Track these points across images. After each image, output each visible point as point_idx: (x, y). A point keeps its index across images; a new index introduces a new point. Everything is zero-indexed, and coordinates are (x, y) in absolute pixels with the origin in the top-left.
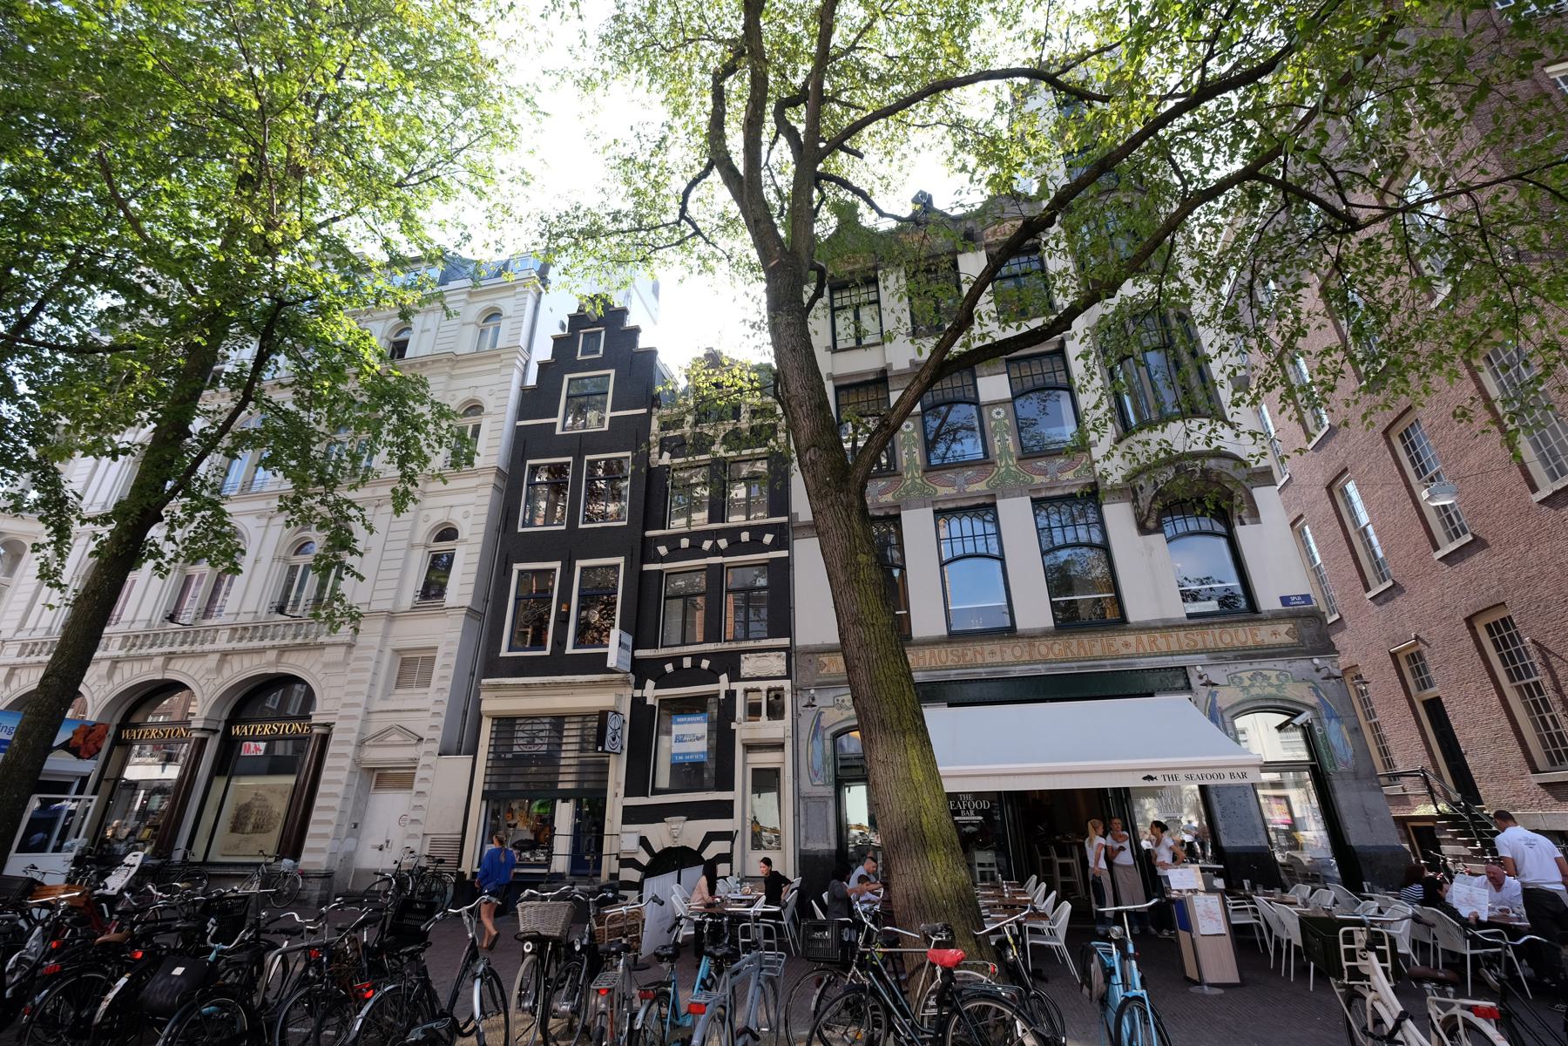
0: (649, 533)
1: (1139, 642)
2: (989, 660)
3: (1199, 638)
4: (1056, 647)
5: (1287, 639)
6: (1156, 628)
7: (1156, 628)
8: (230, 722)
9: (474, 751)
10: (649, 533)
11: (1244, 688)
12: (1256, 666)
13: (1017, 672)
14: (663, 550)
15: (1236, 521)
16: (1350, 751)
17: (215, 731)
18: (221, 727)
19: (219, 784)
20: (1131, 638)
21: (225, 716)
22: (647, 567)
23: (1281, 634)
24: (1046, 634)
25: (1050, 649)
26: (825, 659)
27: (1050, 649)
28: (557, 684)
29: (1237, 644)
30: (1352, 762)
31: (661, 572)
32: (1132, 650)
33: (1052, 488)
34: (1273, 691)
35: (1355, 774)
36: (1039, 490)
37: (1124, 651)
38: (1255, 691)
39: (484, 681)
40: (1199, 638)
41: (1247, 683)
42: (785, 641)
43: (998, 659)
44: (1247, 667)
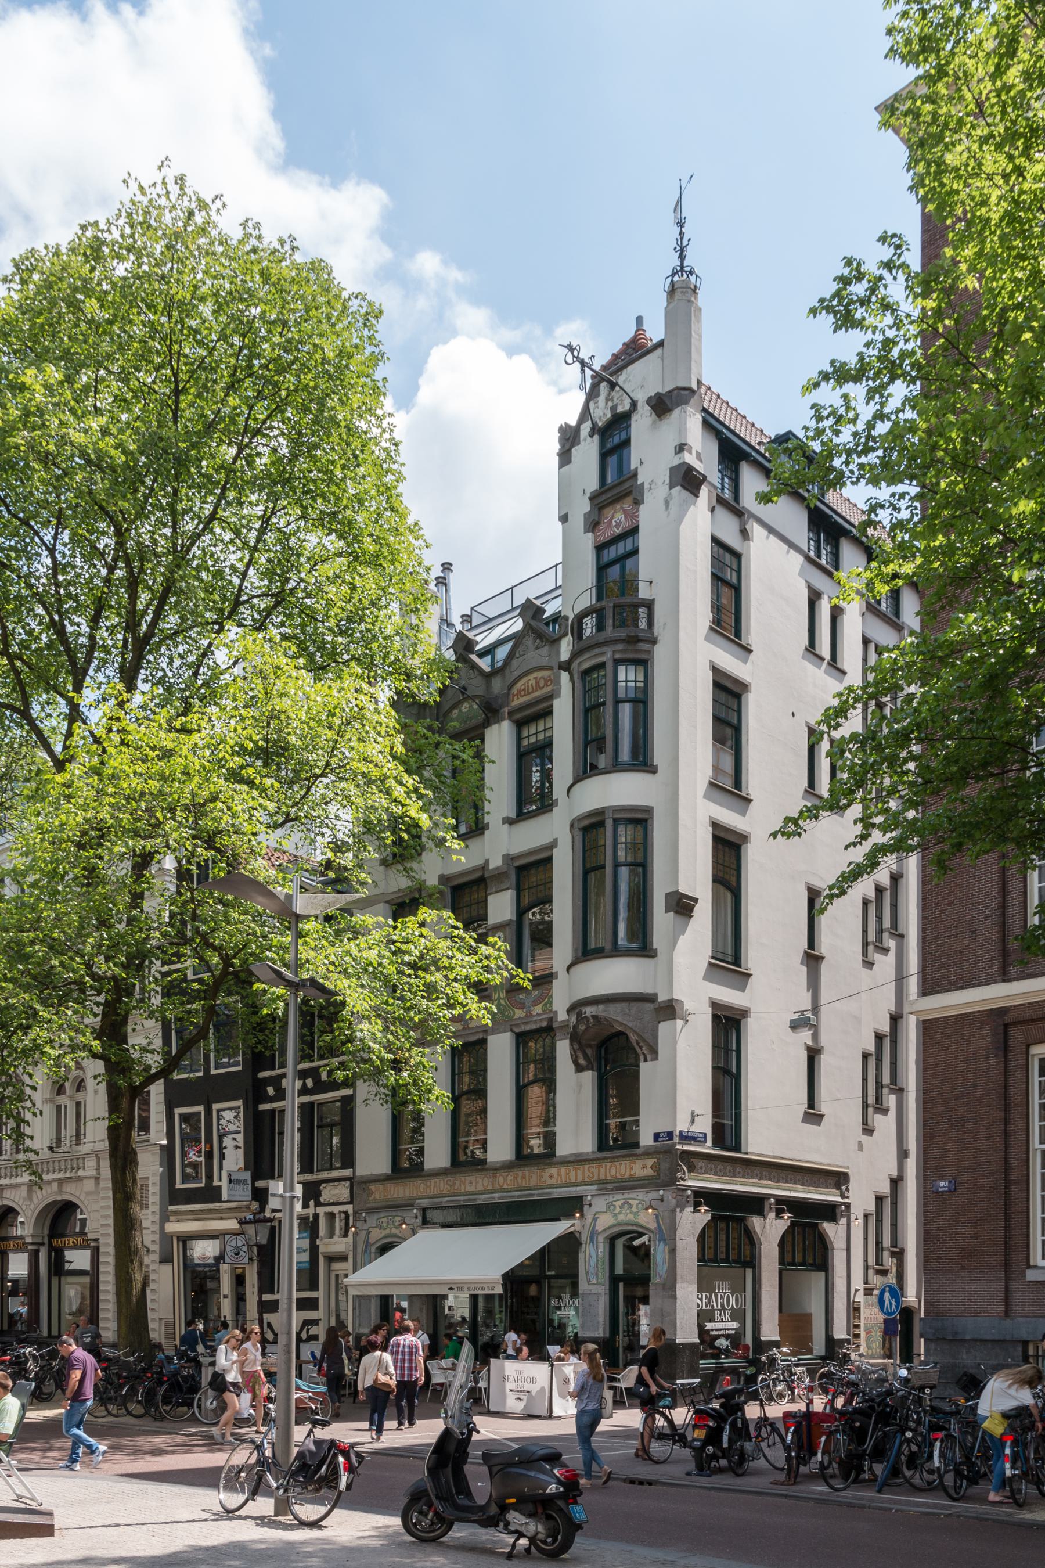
0: (262, 1075)
1: (559, 1174)
2: (469, 1189)
3: (595, 1171)
4: (509, 1178)
5: (649, 1172)
6: (569, 1162)
7: (569, 1162)
8: (52, 1236)
9: (172, 1261)
10: (262, 1075)
11: (615, 1215)
12: (626, 1196)
13: (482, 1199)
14: (271, 1091)
15: (642, 1058)
16: (665, 1267)
17: (43, 1244)
18: (46, 1241)
19: (55, 1281)
20: (554, 1171)
21: (46, 1232)
22: (264, 1107)
23: (642, 1168)
24: (507, 1166)
25: (505, 1180)
26: (372, 1187)
27: (505, 1180)
28: (209, 1211)
29: (619, 1176)
30: (665, 1276)
31: (273, 1111)
32: (553, 1181)
33: (527, 1023)
34: (631, 1217)
35: (664, 1285)
36: (517, 1025)
37: (549, 1182)
38: (622, 1217)
39: (170, 1208)
40: (595, 1171)
41: (618, 1210)
42: (347, 1172)
43: (473, 1188)
44: (620, 1196)
